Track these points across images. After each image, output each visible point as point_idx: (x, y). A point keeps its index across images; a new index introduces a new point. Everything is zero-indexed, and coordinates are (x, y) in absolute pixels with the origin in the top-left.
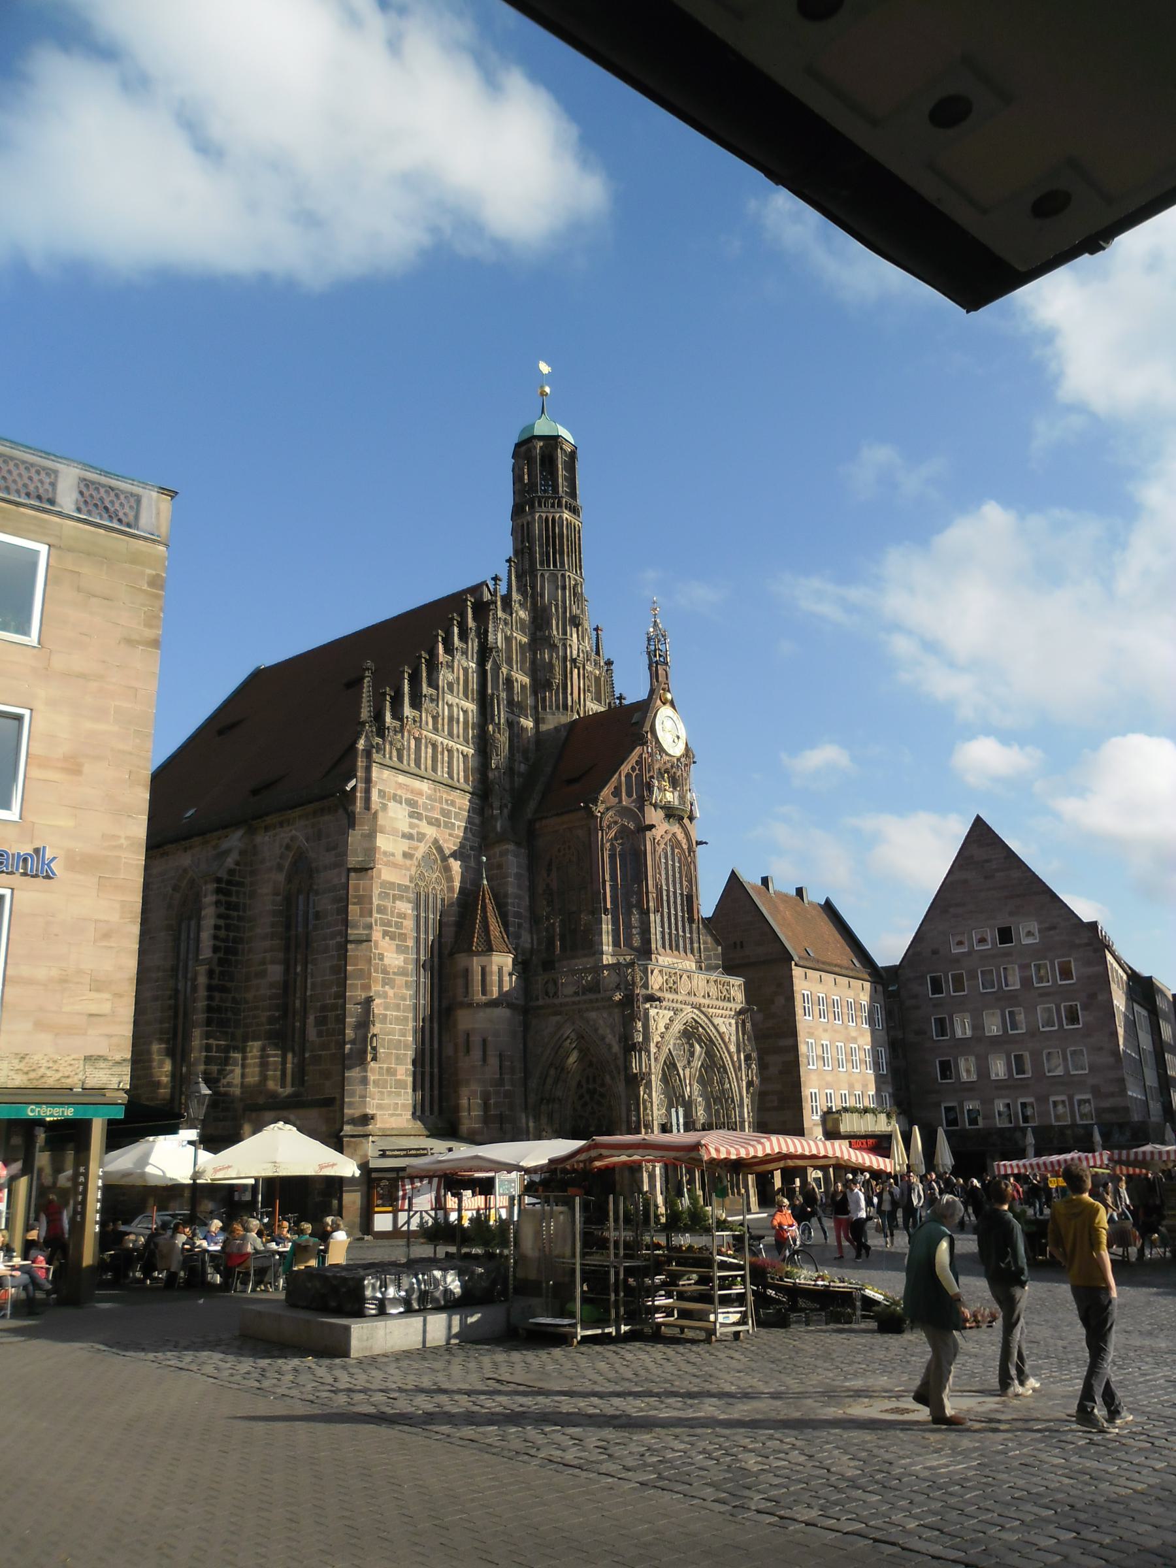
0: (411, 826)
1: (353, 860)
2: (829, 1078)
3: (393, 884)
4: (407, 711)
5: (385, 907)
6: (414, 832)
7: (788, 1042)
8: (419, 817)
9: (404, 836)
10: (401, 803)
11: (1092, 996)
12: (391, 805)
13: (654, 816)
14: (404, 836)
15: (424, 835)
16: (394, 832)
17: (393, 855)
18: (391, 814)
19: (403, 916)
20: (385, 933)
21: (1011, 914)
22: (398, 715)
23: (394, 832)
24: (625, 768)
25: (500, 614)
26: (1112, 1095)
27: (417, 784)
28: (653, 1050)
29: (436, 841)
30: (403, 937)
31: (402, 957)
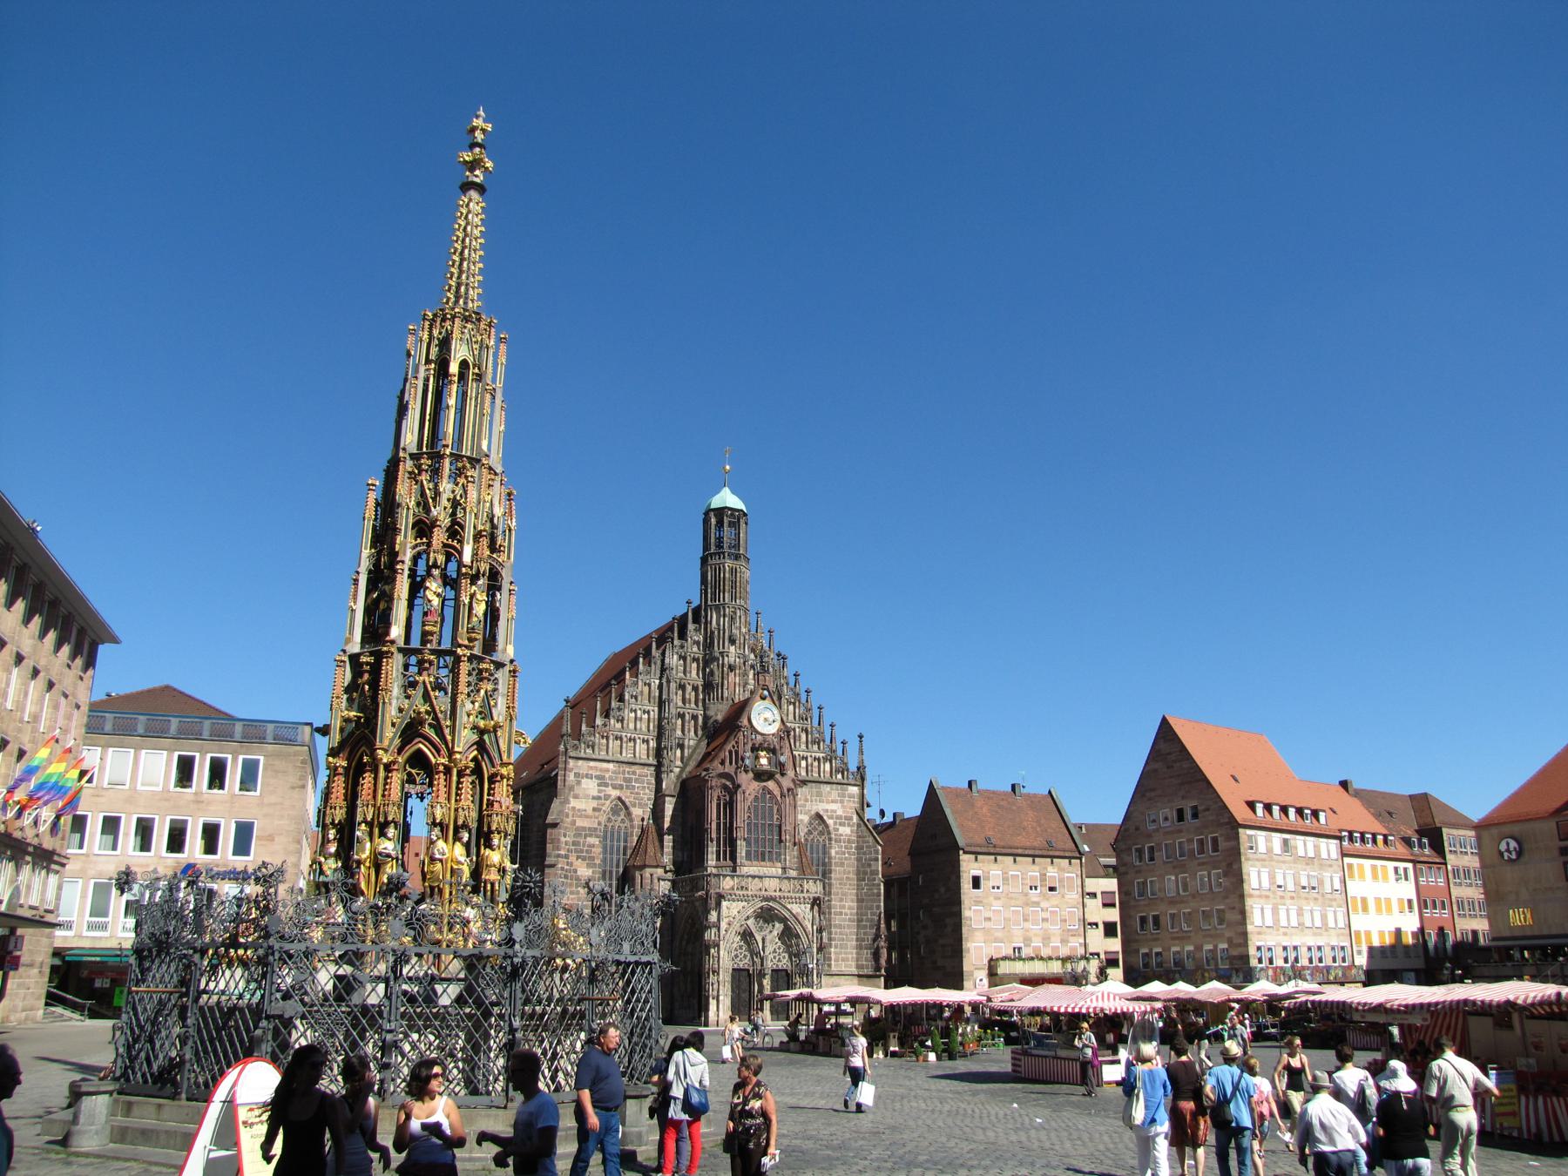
1: (550, 819)
2: (999, 934)
4: (599, 721)
7: (955, 909)
8: (606, 785)
11: (1230, 865)
12: (584, 781)
13: (745, 779)
16: (587, 797)
21: (1183, 798)
22: (592, 725)
23: (587, 797)
24: (729, 747)
25: (676, 642)
26: (1240, 945)
27: (605, 765)
28: (724, 925)
29: (619, 799)
30: (593, 858)
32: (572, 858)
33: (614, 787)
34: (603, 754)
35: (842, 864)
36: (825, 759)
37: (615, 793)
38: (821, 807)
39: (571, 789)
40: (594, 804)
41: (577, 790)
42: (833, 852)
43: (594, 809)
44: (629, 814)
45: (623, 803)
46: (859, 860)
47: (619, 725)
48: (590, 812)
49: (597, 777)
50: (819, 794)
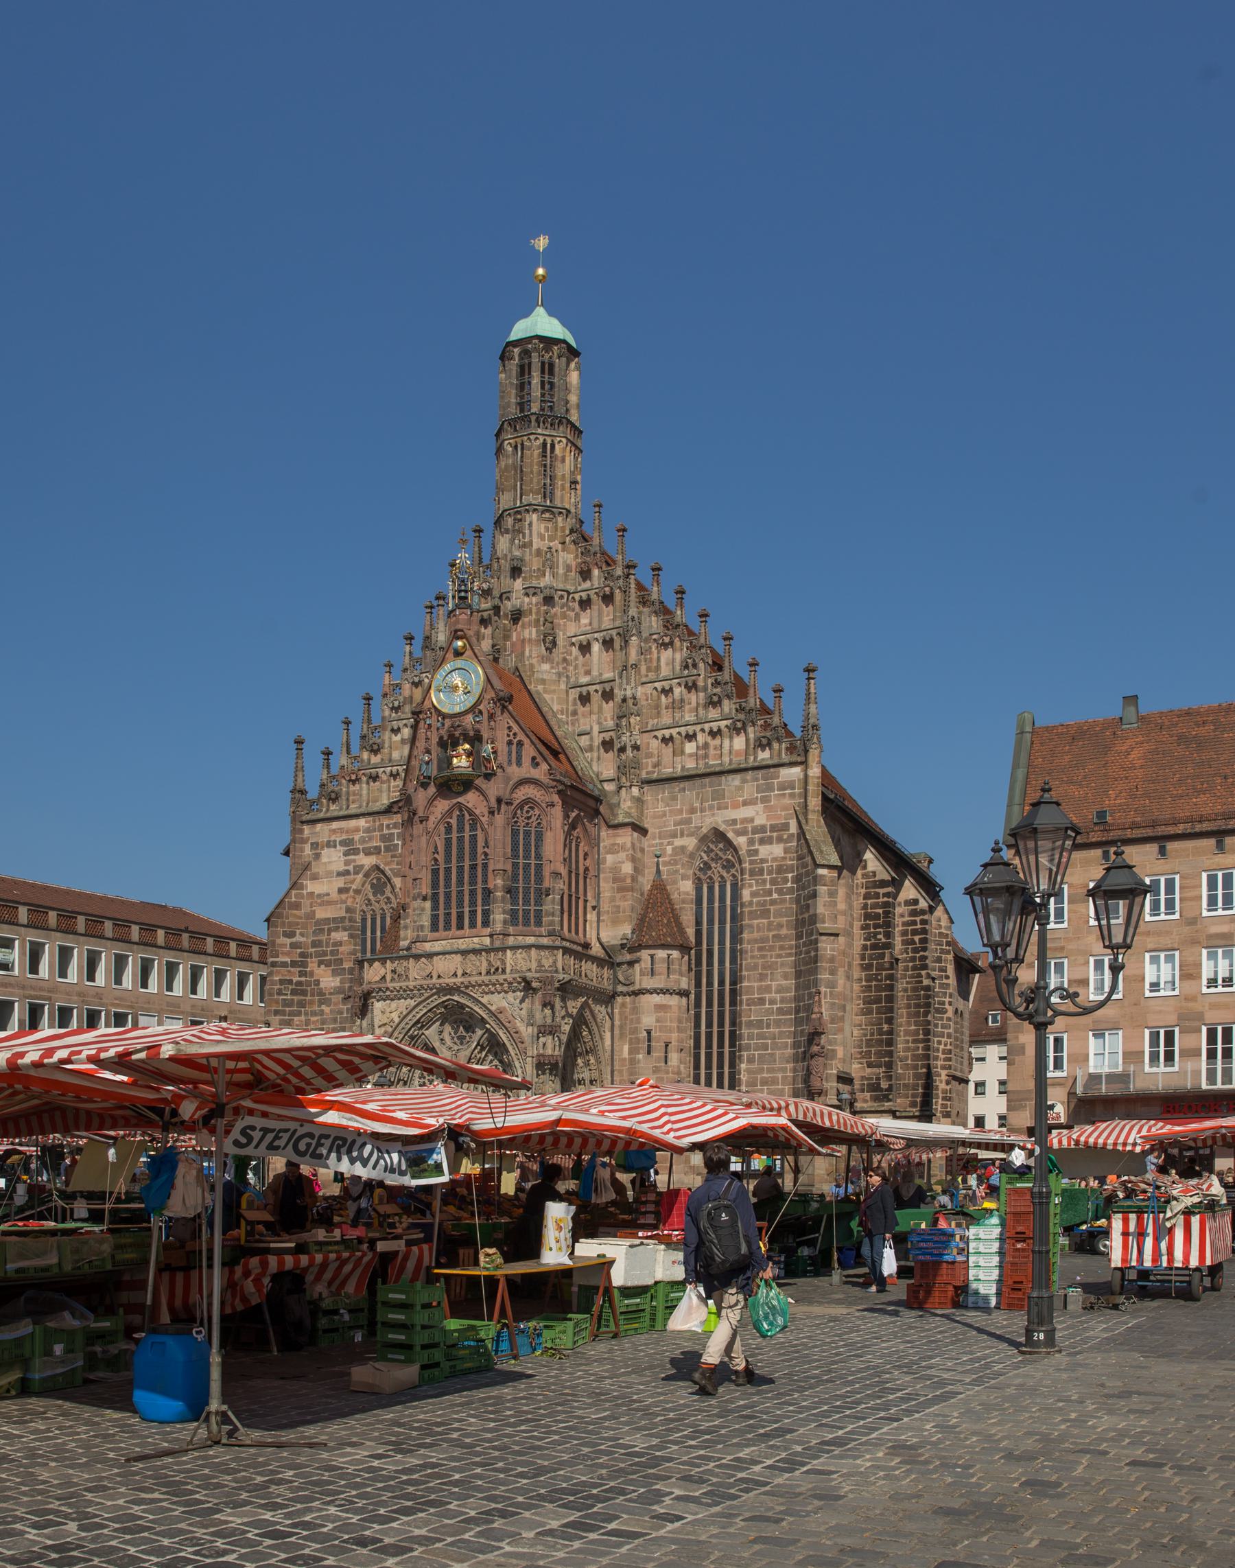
0: (347, 863)
3: (328, 919)
5: (321, 942)
6: (351, 868)
8: (356, 852)
9: (339, 874)
10: (335, 846)
14: (339, 874)
15: (362, 866)
16: (329, 874)
17: (328, 894)
18: (324, 859)
19: (340, 943)
20: (320, 963)
23: (329, 874)
27: (353, 823)
29: (377, 868)
31: (338, 979)
32: (312, 965)
33: (368, 853)
34: (354, 809)
35: (765, 913)
36: (736, 730)
37: (368, 861)
38: (719, 819)
39: (307, 867)
40: (340, 882)
41: (315, 870)
42: (746, 894)
43: (341, 891)
44: (393, 887)
45: (383, 872)
46: (798, 901)
47: (375, 759)
48: (334, 895)
49: (343, 843)
50: (718, 795)
